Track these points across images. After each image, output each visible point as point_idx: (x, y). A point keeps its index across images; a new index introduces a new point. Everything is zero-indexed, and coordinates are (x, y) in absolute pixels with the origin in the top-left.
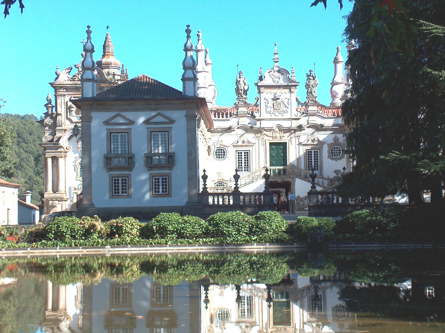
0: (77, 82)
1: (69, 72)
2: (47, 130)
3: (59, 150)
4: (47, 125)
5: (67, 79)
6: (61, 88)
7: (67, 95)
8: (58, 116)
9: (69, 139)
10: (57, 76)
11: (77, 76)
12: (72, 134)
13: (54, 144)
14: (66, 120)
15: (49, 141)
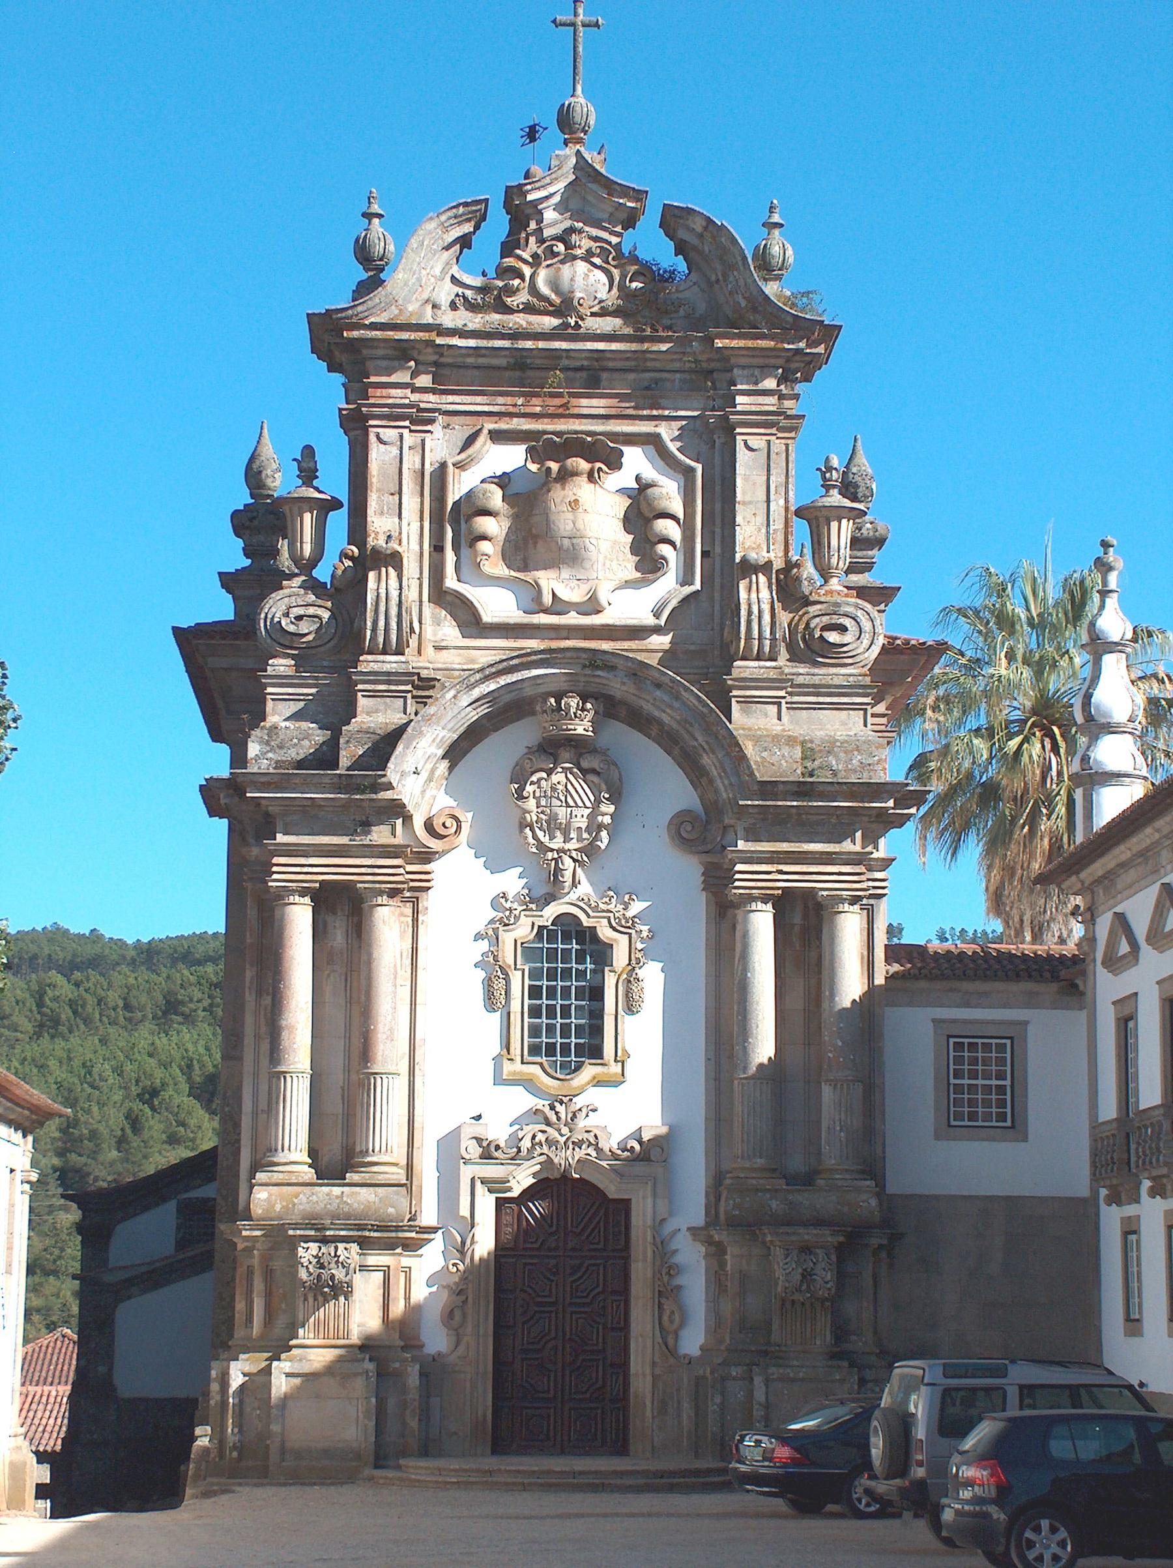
0: (520, 320)
1: (465, 242)
2: (282, 680)
3: (380, 835)
4: (283, 640)
5: (446, 293)
6: (402, 353)
7: (440, 419)
8: (372, 576)
9: (455, 753)
10: (364, 275)
11: (527, 271)
12: (483, 710)
13: (345, 784)
14: (428, 609)
15: (300, 764)
